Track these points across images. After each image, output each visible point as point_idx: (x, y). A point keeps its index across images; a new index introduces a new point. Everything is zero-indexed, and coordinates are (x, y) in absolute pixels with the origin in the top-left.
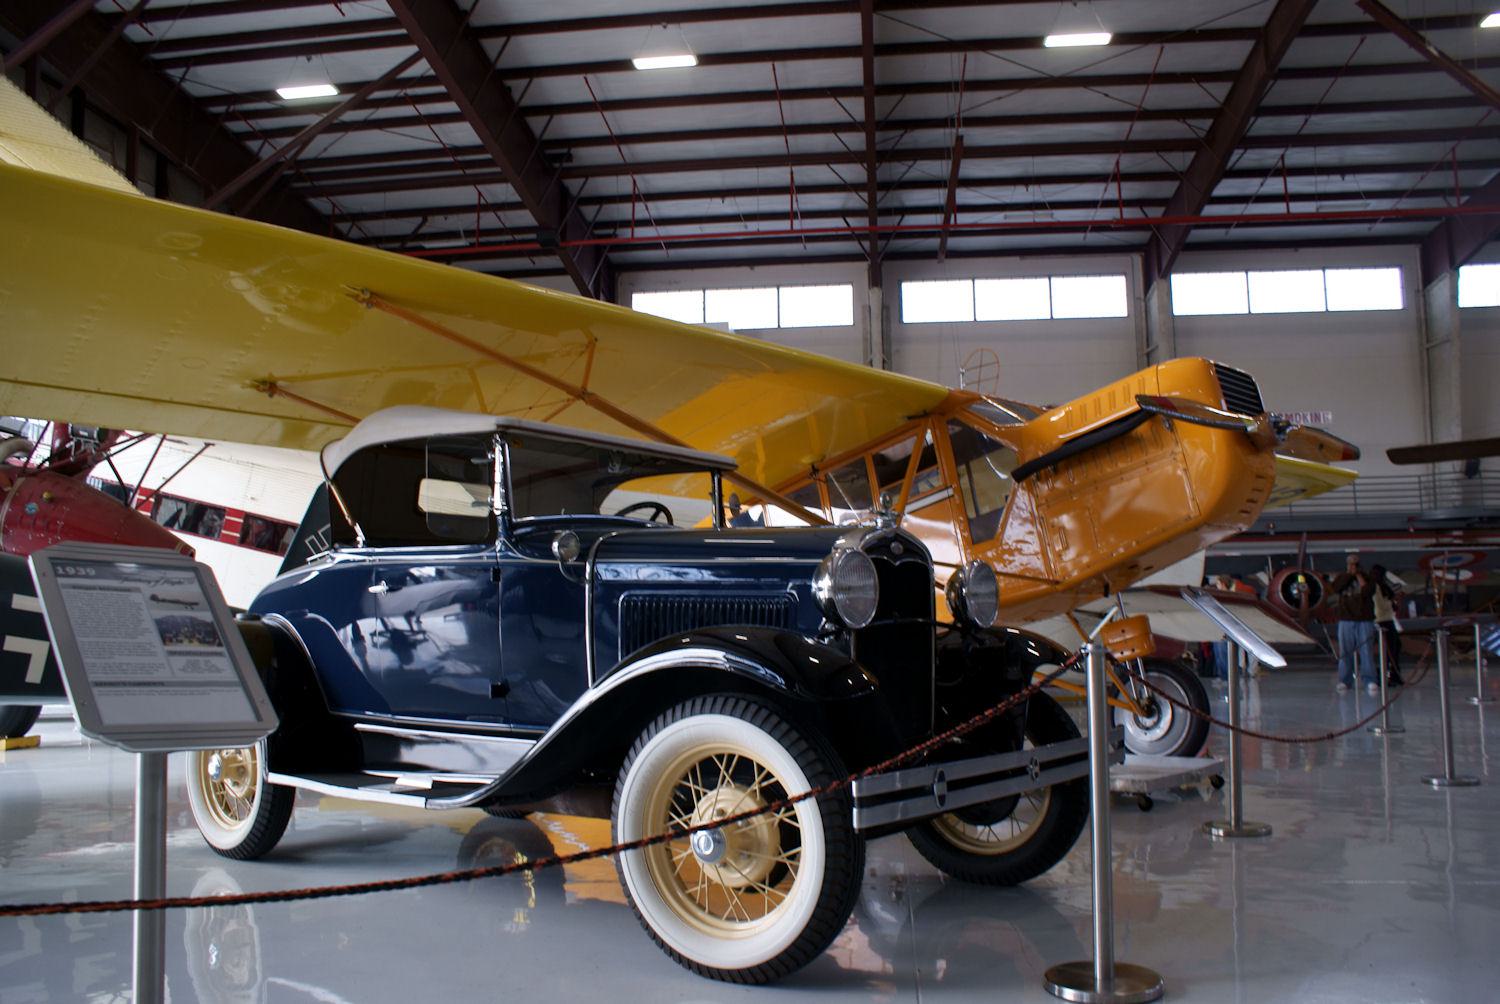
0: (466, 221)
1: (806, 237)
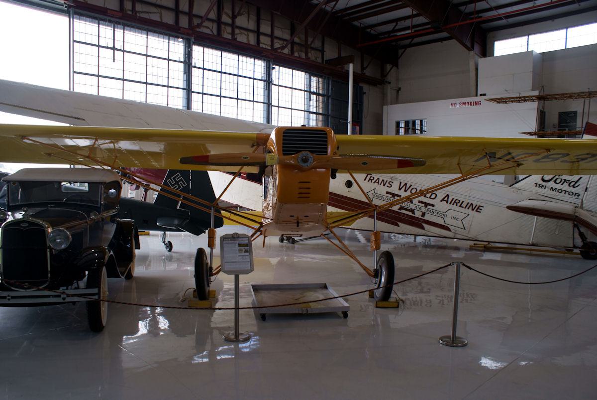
0: (408, 23)
1: (504, 17)
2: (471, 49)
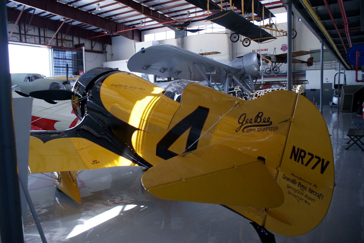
2: (133, 39)
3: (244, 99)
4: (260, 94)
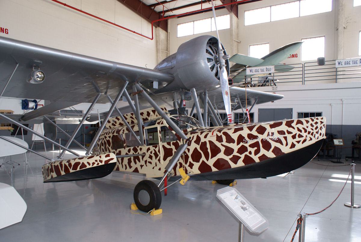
3: (173, 147)
4: (205, 137)
